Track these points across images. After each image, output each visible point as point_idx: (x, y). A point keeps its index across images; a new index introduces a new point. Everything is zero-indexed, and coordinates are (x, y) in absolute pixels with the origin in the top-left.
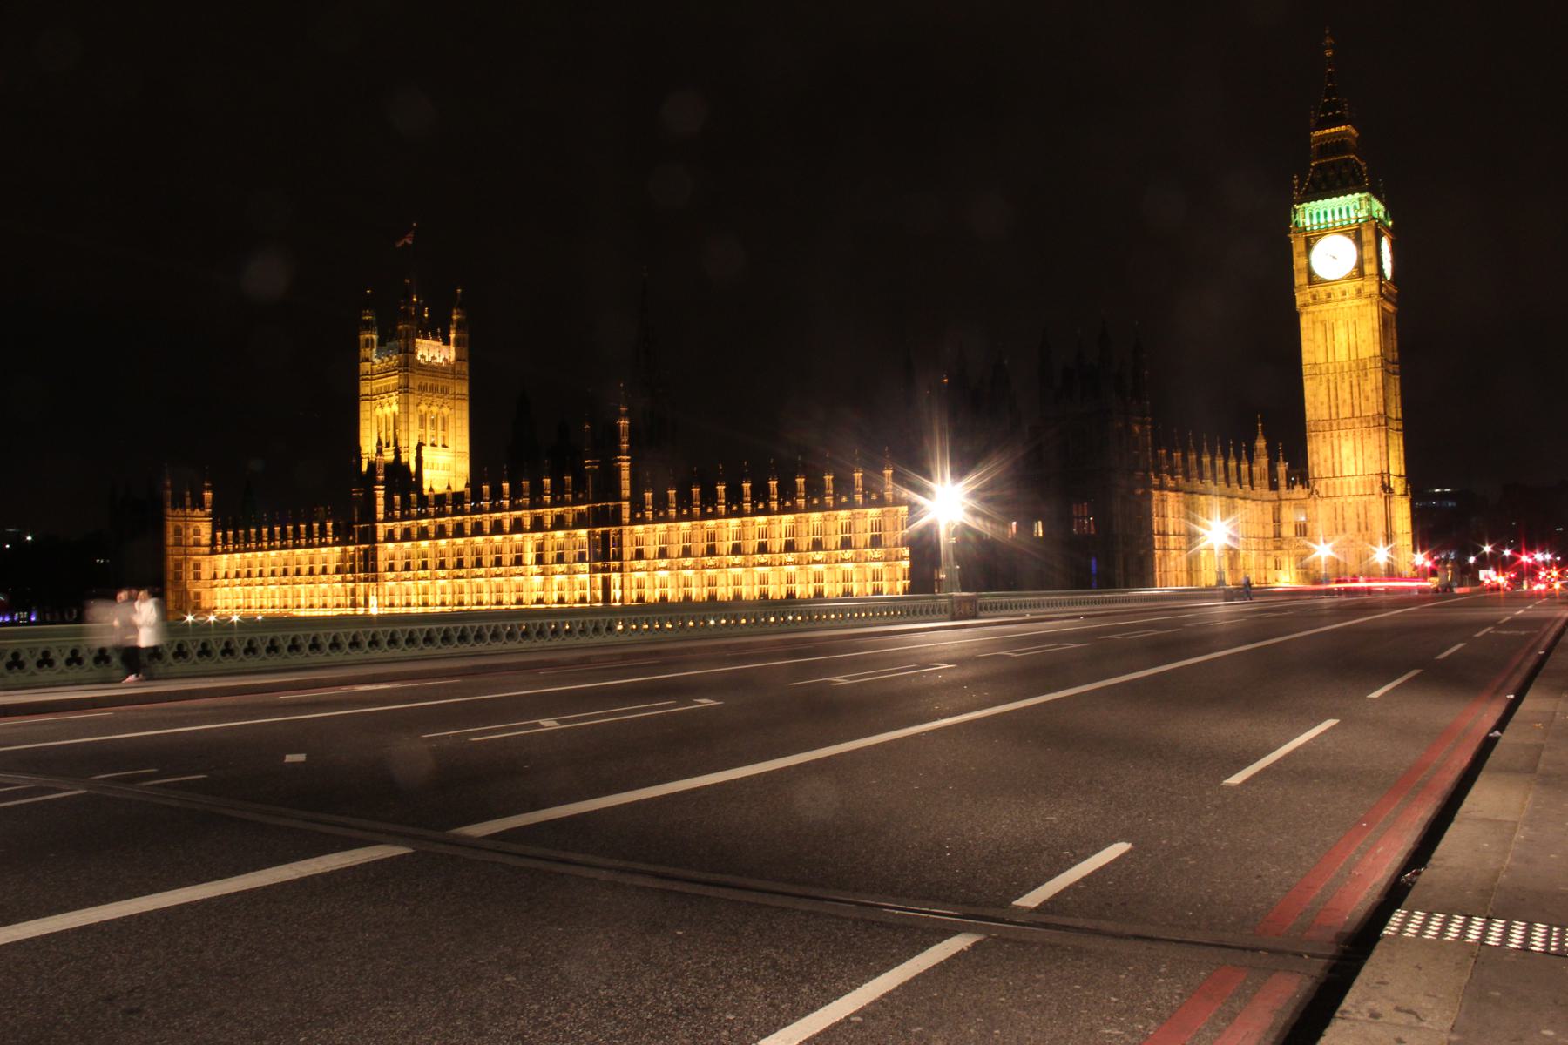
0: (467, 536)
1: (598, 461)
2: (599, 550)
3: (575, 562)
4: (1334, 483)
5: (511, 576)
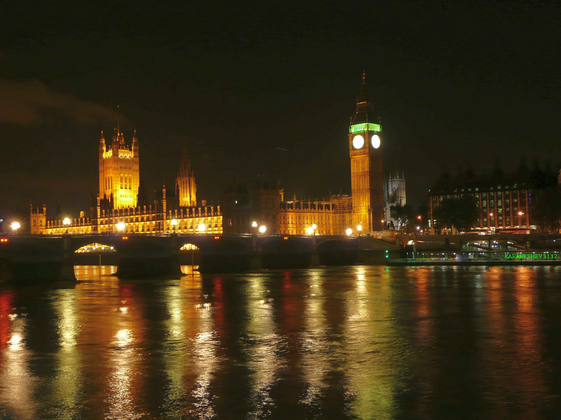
1: (158, 201)
3: (152, 231)
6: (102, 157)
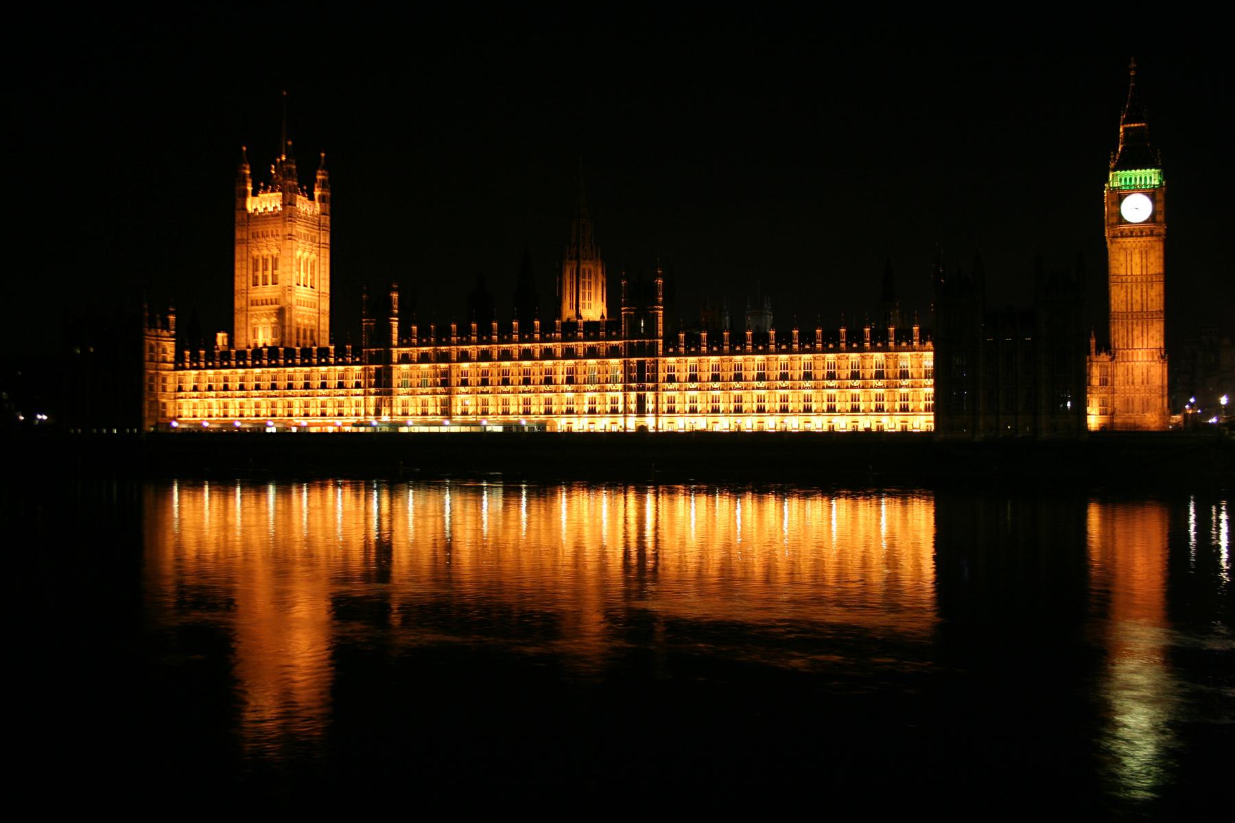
0: (495, 361)
2: (634, 374)
4: (1127, 353)
5: (541, 392)
6: (245, 209)
